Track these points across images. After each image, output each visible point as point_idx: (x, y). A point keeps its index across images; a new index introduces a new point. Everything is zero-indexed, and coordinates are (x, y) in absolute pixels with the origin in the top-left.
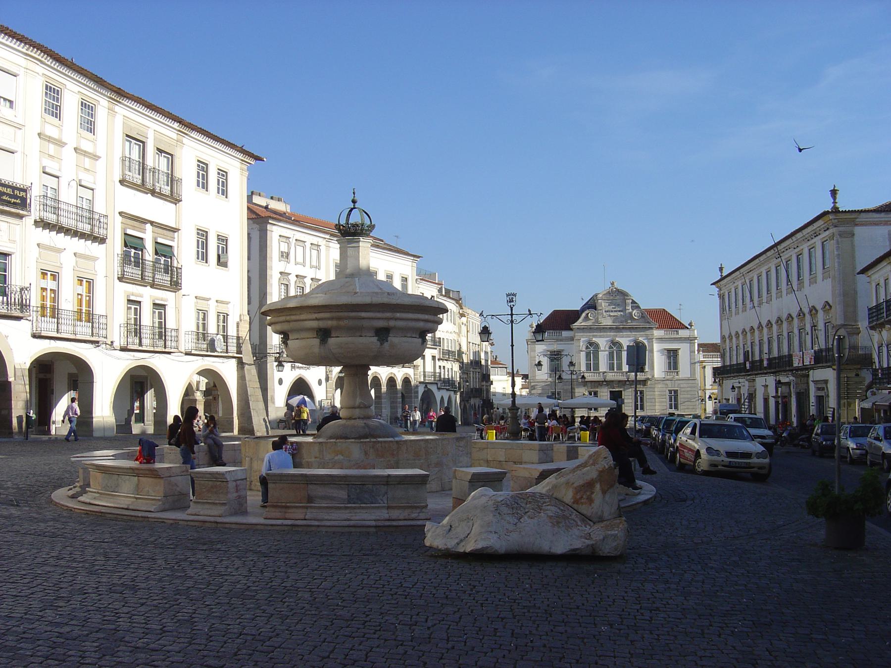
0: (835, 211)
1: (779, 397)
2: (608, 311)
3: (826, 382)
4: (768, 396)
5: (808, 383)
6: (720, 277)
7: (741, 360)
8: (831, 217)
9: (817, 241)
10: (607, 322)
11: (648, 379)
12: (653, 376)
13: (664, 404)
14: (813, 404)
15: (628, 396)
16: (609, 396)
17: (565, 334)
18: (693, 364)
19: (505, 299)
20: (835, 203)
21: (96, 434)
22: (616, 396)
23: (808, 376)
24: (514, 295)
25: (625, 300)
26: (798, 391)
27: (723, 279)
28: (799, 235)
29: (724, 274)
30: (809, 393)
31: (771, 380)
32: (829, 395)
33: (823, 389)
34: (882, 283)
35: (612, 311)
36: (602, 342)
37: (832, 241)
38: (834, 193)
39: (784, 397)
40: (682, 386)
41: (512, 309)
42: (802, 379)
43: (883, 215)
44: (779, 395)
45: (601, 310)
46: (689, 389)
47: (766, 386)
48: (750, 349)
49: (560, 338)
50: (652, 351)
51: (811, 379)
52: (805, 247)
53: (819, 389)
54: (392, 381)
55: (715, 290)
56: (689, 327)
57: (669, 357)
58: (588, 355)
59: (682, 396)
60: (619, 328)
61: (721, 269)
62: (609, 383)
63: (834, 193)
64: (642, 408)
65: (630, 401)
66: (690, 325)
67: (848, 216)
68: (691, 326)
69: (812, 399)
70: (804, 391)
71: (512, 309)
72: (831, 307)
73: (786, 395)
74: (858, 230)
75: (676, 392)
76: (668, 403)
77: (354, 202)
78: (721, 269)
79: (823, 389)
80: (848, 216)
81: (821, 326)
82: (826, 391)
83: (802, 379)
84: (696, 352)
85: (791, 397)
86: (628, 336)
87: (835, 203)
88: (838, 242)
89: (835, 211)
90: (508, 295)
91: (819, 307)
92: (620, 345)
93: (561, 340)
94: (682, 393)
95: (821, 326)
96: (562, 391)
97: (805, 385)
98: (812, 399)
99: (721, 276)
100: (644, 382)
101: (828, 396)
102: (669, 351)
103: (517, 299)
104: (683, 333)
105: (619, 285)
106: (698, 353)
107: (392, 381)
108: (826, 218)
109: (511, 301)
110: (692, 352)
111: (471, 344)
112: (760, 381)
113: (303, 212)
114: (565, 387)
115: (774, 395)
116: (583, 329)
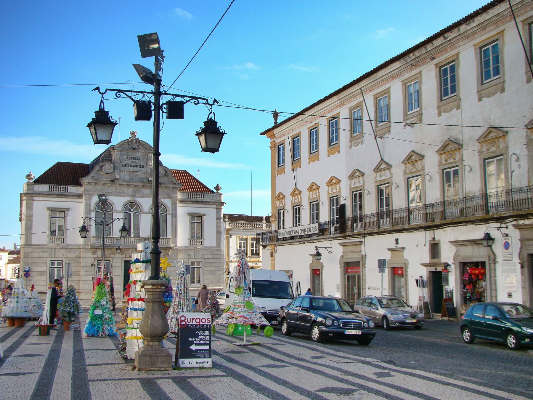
2: (126, 166)
6: (274, 124)
12: (176, 245)
16: (123, 268)
17: (72, 189)
18: (219, 233)
29: (279, 121)
35: (131, 166)
40: (206, 257)
46: (213, 261)
49: (66, 193)
50: (174, 216)
55: (266, 141)
56: (215, 191)
57: (192, 222)
59: (205, 269)
61: (276, 115)
66: (217, 188)
84: (222, 220)
85: (495, 262)
93: (67, 196)
96: (64, 260)
99: (276, 123)
104: (208, 198)
114: (70, 255)
115: (427, 260)
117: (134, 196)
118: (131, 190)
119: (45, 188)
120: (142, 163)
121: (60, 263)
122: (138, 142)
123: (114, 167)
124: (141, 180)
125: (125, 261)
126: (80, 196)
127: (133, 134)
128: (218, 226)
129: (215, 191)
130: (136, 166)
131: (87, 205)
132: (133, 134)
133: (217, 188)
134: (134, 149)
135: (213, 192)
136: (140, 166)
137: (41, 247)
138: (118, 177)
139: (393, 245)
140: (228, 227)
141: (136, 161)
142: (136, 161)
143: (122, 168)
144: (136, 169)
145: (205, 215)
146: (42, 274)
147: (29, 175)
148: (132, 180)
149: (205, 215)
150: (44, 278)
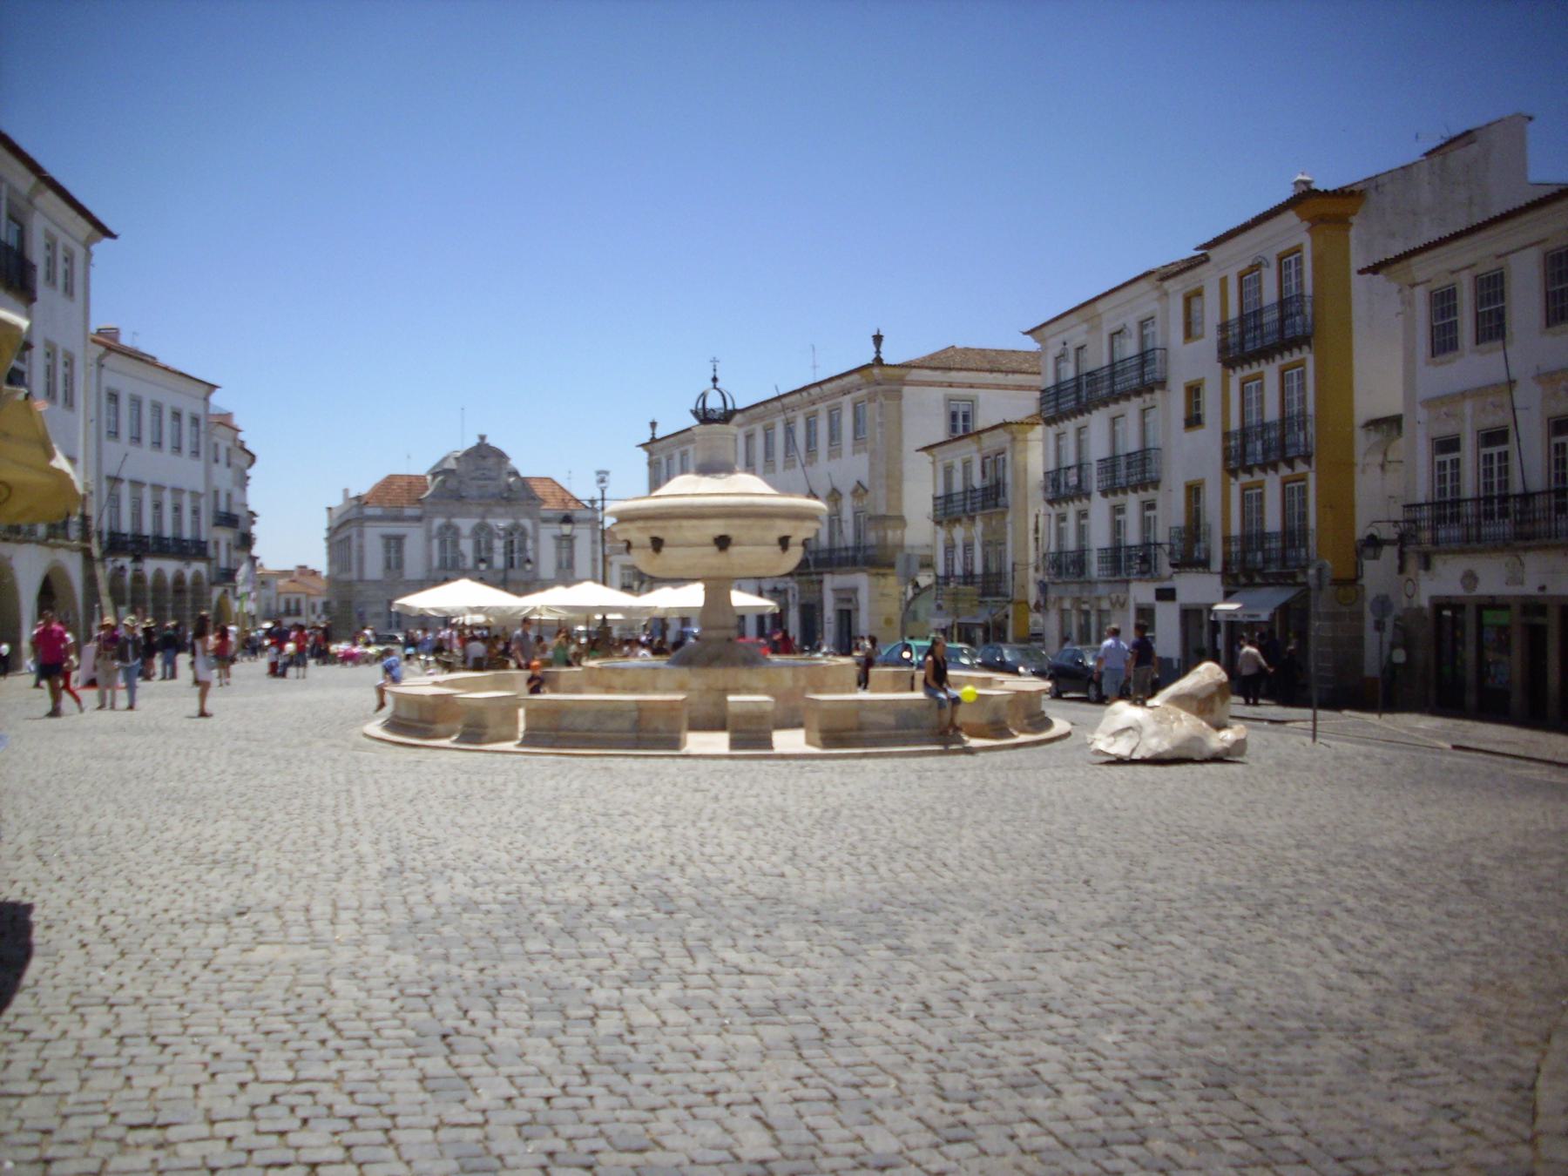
0: (878, 361)
2: (473, 479)
5: (821, 591)
8: (876, 371)
9: (846, 402)
19: (594, 478)
20: (878, 352)
23: (821, 582)
24: (606, 473)
27: (653, 440)
28: (816, 391)
33: (849, 600)
34: (958, 465)
36: (466, 525)
37: (873, 405)
38: (878, 339)
41: (603, 492)
43: (938, 373)
50: (536, 540)
52: (822, 408)
54: (179, 579)
55: (643, 455)
57: (559, 547)
58: (443, 544)
61: (653, 425)
63: (878, 339)
67: (897, 372)
71: (603, 492)
72: (866, 491)
74: (906, 390)
77: (715, 380)
78: (653, 425)
79: (849, 600)
80: (897, 372)
81: (847, 514)
86: (502, 516)
87: (878, 352)
88: (881, 405)
89: (878, 361)
90: (599, 473)
91: (846, 489)
92: (491, 533)
95: (847, 514)
101: (857, 609)
103: (612, 479)
105: (491, 441)
107: (179, 579)
108: (866, 372)
109: (602, 481)
117: (483, 517)
118: (480, 510)
120: (493, 474)
122: (487, 446)
123: (460, 482)
124: (493, 496)
126: (419, 519)
127: (482, 438)
131: (429, 531)
132: (482, 438)
134: (484, 458)
136: (490, 479)
137: (375, 582)
138: (464, 494)
148: (481, 497)
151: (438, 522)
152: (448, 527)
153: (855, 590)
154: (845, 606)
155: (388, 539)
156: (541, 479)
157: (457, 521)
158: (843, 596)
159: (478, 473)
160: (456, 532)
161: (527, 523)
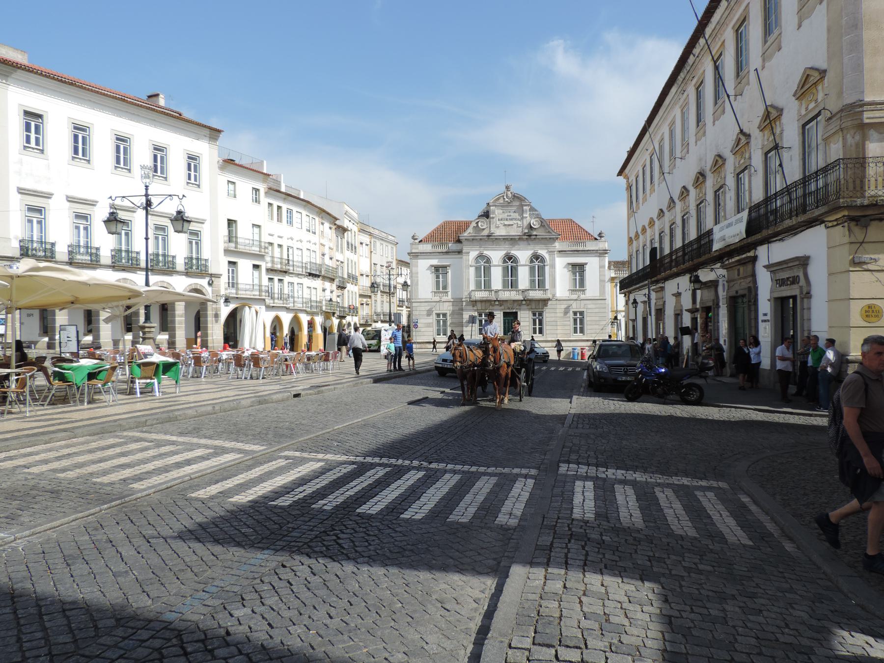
1: (697, 310)
3: (803, 262)
4: (681, 310)
5: (754, 275)
7: (648, 262)
10: (501, 232)
11: (549, 300)
13: (567, 328)
14: (768, 317)
15: (525, 319)
21: (28, 361)
22: (511, 318)
25: (522, 206)
26: (733, 293)
30: (756, 295)
31: (683, 283)
32: (813, 292)
33: (795, 280)
35: (507, 220)
39: (707, 310)
42: (741, 269)
44: (698, 306)
45: (493, 218)
46: (597, 310)
47: (678, 295)
48: (657, 245)
50: (553, 266)
51: (762, 261)
53: (782, 283)
56: (598, 238)
60: (515, 239)
62: (501, 302)
64: (541, 332)
65: (527, 324)
66: (600, 235)
68: (601, 237)
69: (765, 306)
70: (746, 292)
73: (710, 304)
75: (582, 313)
76: (572, 326)
79: (795, 280)
82: (802, 282)
83: (741, 269)
94: (588, 315)
97: (750, 279)
98: (765, 306)
100: (545, 302)
101: (808, 295)
102: (574, 266)
104: (591, 246)
106: (609, 268)
110: (602, 267)
111: (378, 267)
112: (671, 286)
113: (36, 65)
115: (690, 306)
116: (472, 240)
119: (427, 247)
121: (445, 315)
125: (504, 313)
126: (460, 252)
128: (602, 275)
129: (598, 238)
130: (512, 220)
133: (600, 235)
135: (596, 239)
136: (515, 219)
139: (675, 291)
140: (613, 275)
141: (512, 214)
142: (512, 214)
143: (498, 223)
144: (511, 222)
145: (586, 264)
146: (429, 325)
147: (413, 236)
149: (586, 264)
150: (431, 329)
151: (473, 254)
152: (481, 256)
153: (803, 262)
154: (786, 292)
155: (437, 269)
156: (563, 221)
157: (486, 253)
158: (784, 275)
159: (505, 216)
160: (488, 260)
161: (543, 252)
